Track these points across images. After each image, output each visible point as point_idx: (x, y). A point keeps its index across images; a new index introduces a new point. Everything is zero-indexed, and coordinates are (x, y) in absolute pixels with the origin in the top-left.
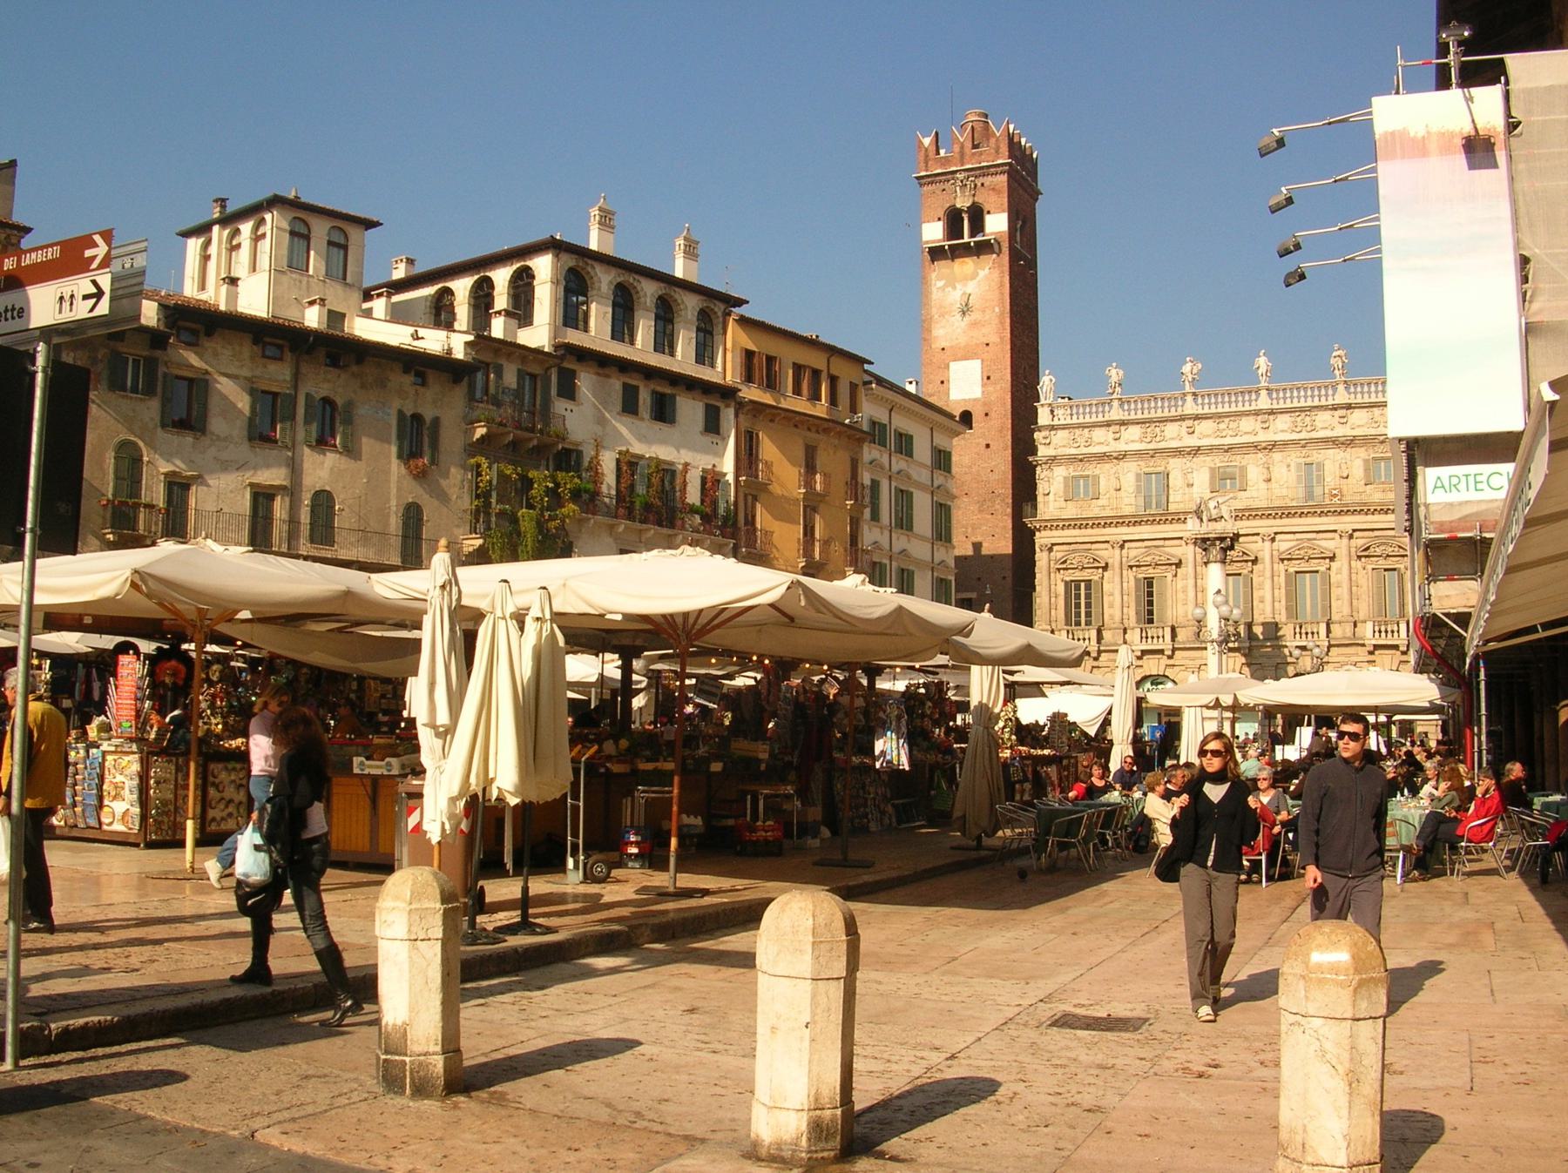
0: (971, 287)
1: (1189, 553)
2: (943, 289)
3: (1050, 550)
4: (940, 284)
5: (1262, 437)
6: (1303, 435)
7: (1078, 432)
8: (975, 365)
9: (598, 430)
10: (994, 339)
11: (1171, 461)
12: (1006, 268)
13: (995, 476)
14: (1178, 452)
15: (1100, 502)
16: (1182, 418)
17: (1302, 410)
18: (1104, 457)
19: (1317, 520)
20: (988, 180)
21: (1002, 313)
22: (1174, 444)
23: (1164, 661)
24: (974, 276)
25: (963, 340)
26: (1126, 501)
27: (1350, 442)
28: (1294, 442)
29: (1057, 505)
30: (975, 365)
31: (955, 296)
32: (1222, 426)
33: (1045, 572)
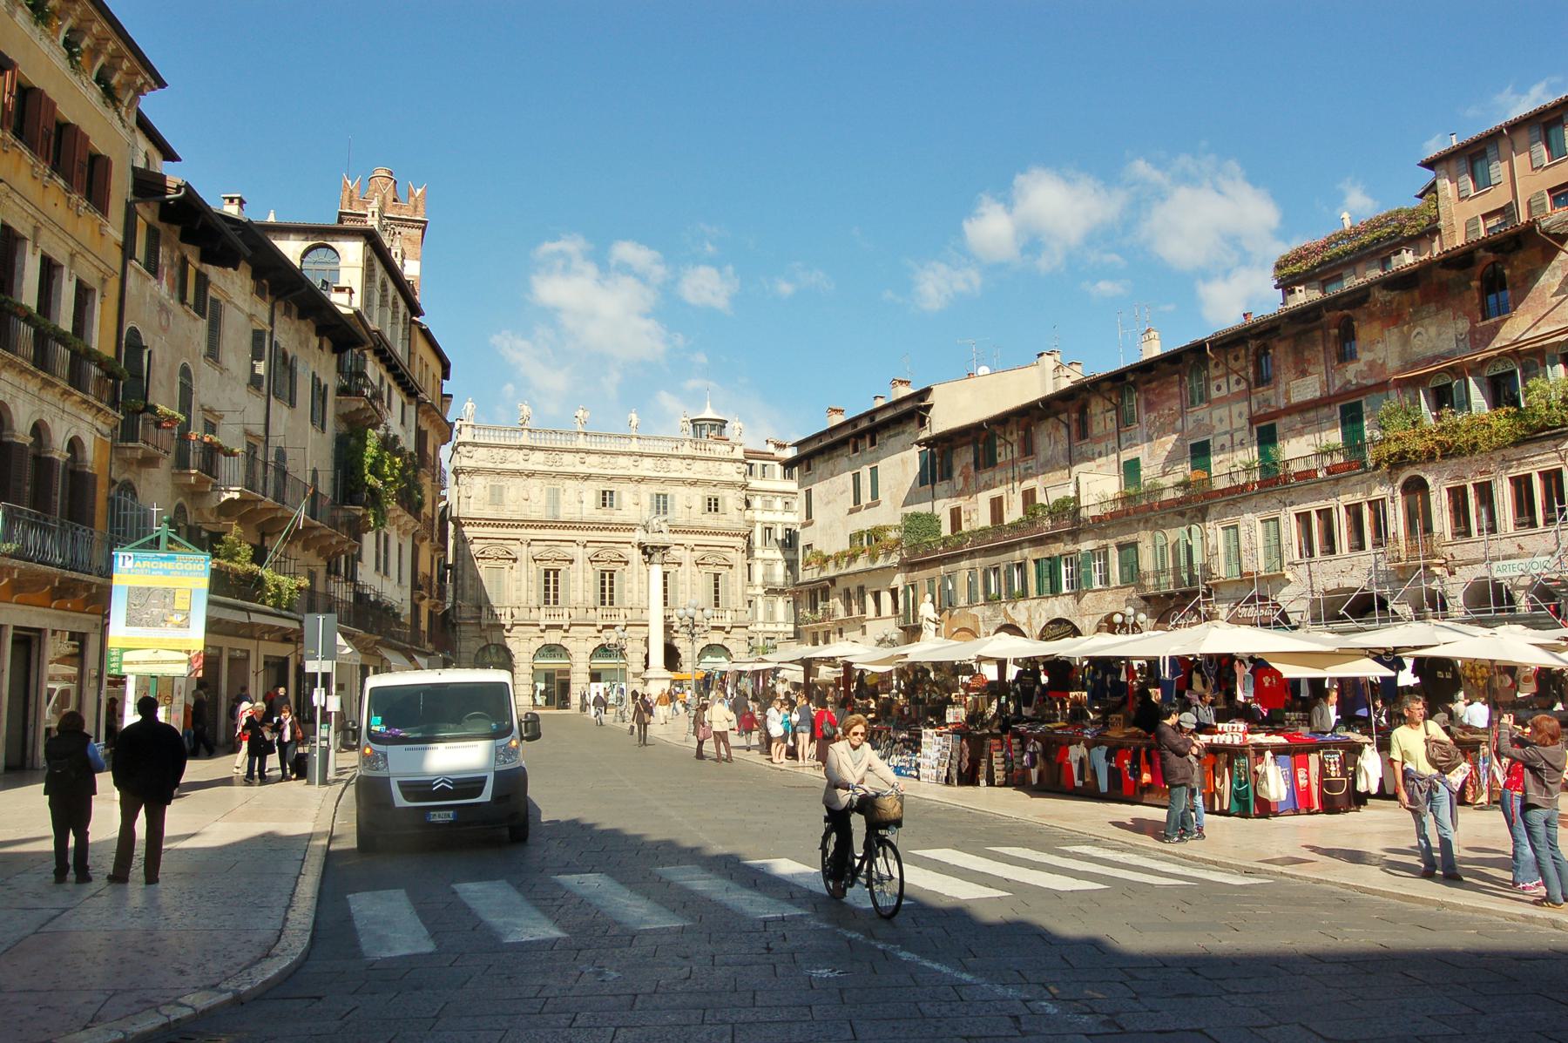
1: (636, 555)
5: (633, 472)
14: (574, 476)
20: (405, 231)
22: (570, 469)
23: (561, 633)
28: (657, 479)
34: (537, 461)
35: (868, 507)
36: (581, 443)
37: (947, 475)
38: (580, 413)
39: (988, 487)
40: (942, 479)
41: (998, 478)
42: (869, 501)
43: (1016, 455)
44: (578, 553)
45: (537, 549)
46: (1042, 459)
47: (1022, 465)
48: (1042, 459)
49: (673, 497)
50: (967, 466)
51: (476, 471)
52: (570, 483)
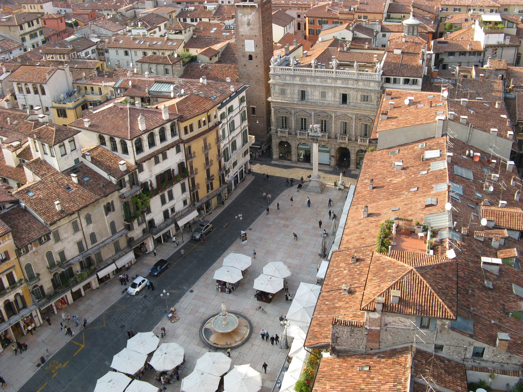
0: (250, 17)
2: (241, 16)
4: (240, 15)
6: (345, 86)
8: (252, 42)
9: (150, 173)
10: (257, 34)
12: (260, 12)
13: (259, 75)
18: (288, 84)
21: (260, 27)
24: (251, 14)
25: (248, 34)
27: (358, 90)
30: (252, 42)
31: (245, 19)
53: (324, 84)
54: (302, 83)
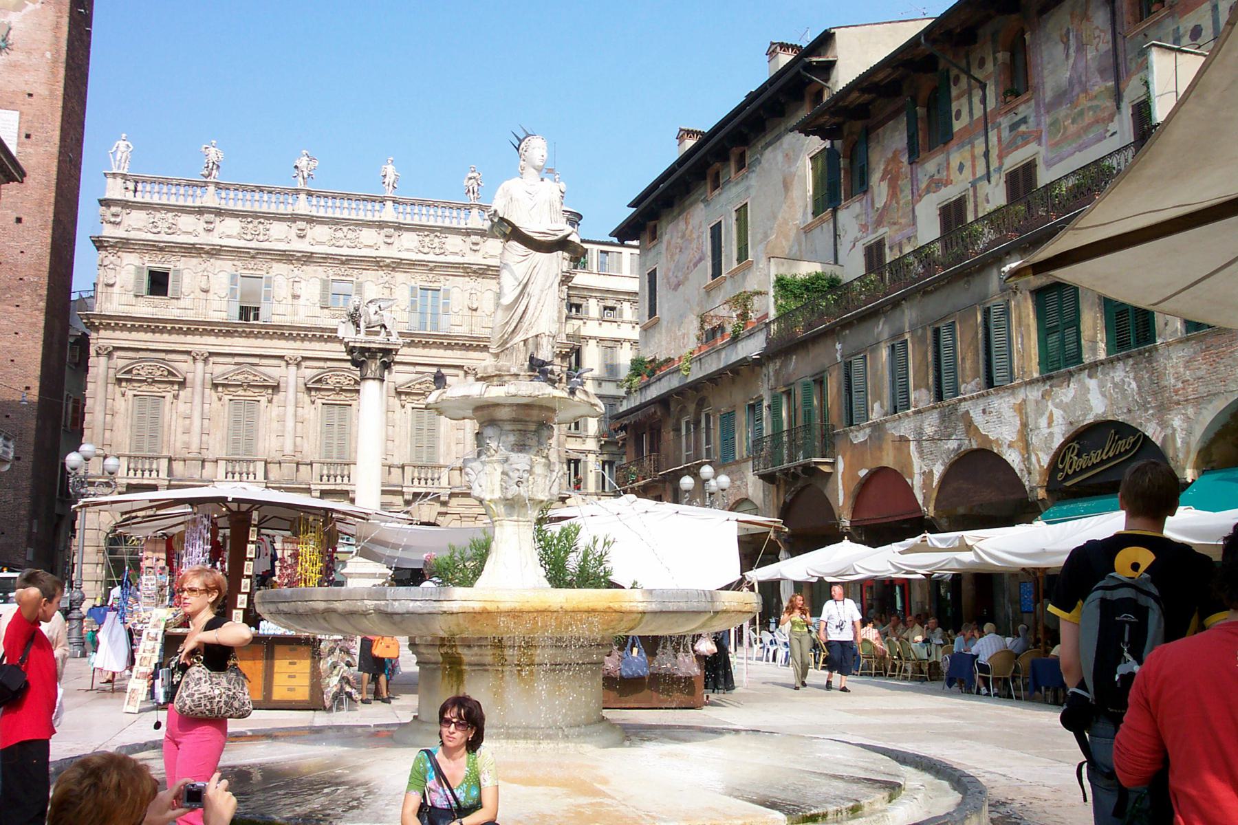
3: (110, 355)
5: (384, 252)
7: (163, 214)
10: (41, 90)
11: (275, 265)
14: (286, 257)
15: (182, 303)
16: (294, 218)
17: (432, 229)
19: (441, 352)
21: (55, 61)
26: (216, 305)
28: (422, 264)
29: (124, 299)
32: (339, 234)
33: (101, 382)
34: (228, 232)
35: (733, 275)
36: (302, 206)
37: (861, 185)
38: (303, 162)
39: (936, 184)
40: (850, 195)
41: (954, 163)
42: (735, 265)
43: (991, 103)
44: (291, 377)
45: (219, 369)
46: (1048, 95)
47: (1005, 122)
48: (1048, 95)
49: (447, 291)
50: (895, 158)
51: (124, 245)
52: (280, 270)
53: (345, 251)
54: (254, 244)
